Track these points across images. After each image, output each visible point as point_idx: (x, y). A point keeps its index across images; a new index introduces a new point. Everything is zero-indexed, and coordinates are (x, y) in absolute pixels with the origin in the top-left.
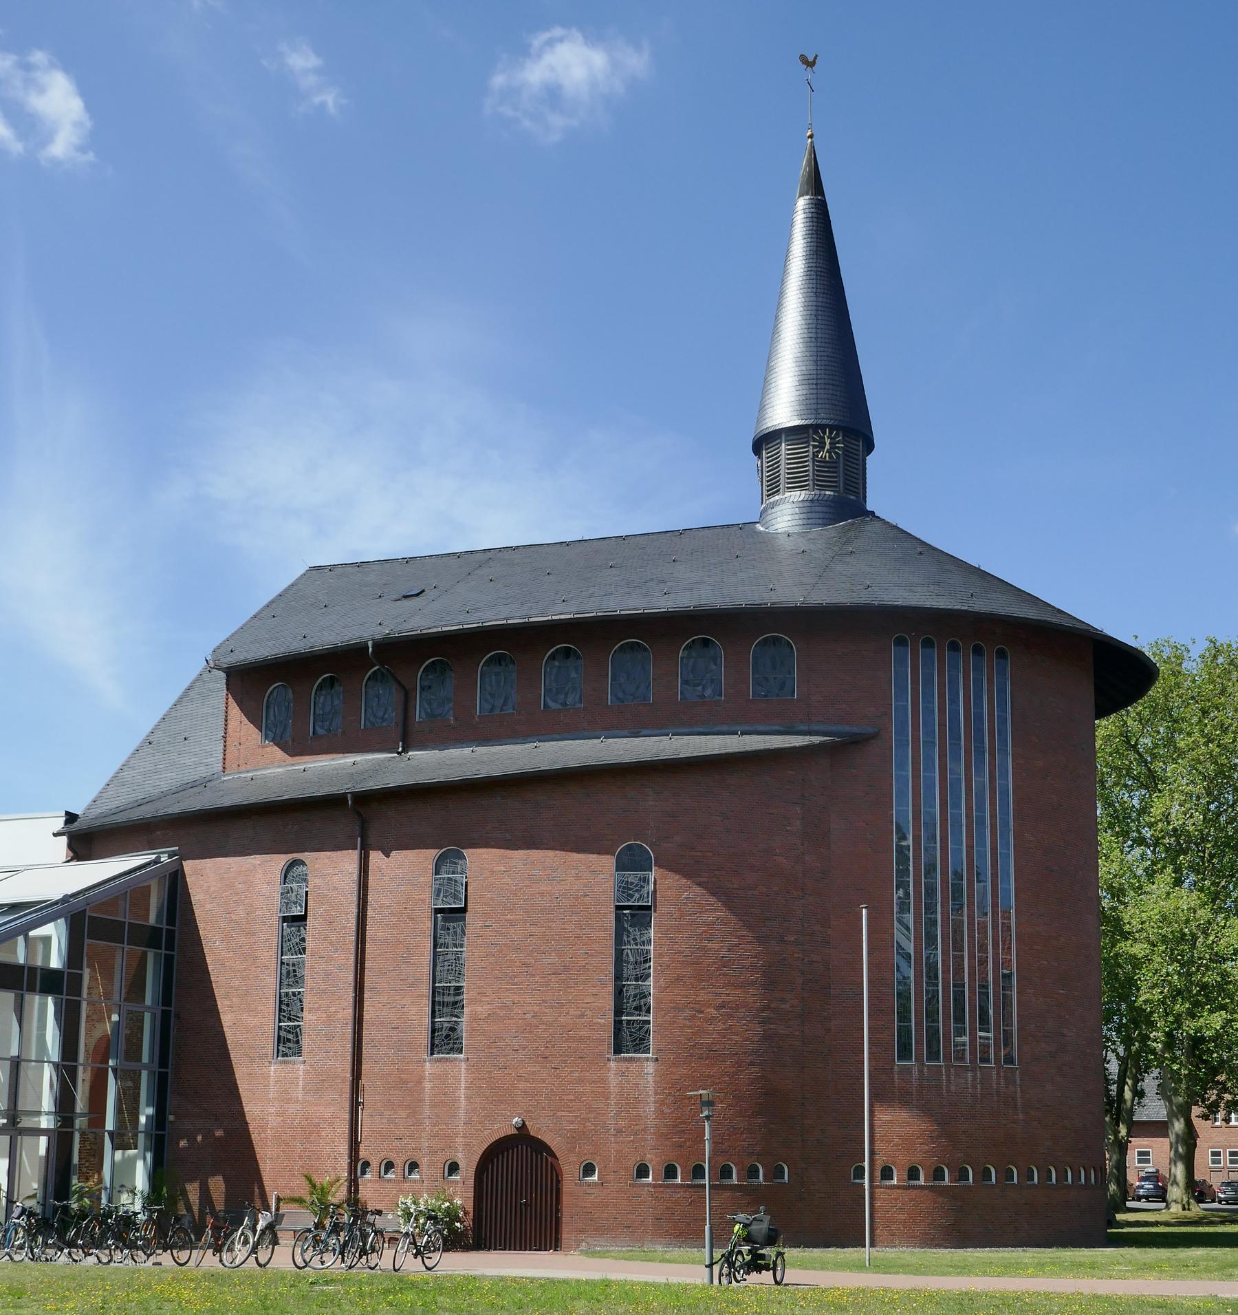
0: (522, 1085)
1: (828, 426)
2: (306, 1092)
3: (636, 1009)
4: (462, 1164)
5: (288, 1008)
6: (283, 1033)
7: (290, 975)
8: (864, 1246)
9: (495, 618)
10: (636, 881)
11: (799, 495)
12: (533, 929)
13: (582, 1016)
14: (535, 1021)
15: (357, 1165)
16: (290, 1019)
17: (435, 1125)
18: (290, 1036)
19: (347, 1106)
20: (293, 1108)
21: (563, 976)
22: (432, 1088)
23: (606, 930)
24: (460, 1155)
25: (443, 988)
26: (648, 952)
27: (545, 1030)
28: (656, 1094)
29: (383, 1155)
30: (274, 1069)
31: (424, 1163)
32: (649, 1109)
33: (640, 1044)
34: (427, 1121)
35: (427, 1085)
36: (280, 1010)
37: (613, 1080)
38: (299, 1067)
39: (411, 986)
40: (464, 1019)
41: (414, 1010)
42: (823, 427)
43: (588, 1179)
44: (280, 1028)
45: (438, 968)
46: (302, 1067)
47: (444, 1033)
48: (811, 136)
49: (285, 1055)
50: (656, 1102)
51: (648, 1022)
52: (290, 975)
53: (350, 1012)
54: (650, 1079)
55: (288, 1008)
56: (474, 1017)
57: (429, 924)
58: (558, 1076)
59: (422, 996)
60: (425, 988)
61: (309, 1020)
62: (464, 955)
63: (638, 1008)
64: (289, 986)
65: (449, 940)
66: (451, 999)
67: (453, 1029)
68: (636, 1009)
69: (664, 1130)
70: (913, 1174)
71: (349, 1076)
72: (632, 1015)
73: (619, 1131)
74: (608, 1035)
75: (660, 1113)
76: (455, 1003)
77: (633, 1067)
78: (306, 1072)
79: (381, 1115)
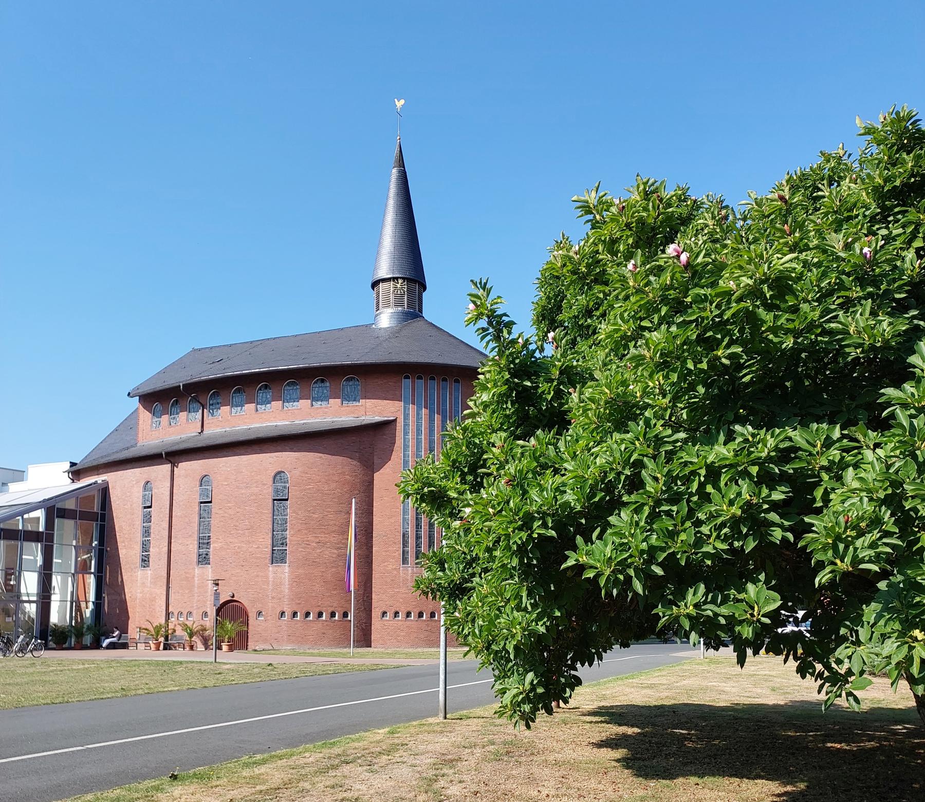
0: (233, 578)
1: (400, 278)
2: (151, 583)
3: (281, 544)
4: (209, 614)
5: (145, 547)
6: (144, 558)
7: (147, 532)
8: (439, 646)
9: (257, 367)
10: (281, 488)
11: (390, 311)
12: (238, 510)
13: (258, 547)
14: (239, 550)
15: (168, 615)
16: (146, 551)
17: (199, 596)
18: (146, 559)
19: (165, 588)
20: (146, 590)
21: (250, 530)
22: (198, 580)
23: (268, 510)
24: (208, 609)
25: (203, 536)
26: (287, 519)
27: (243, 554)
28: (289, 581)
29: (179, 610)
30: (140, 573)
31: (194, 612)
32: (286, 590)
33: (283, 560)
34: (196, 595)
35: (196, 579)
36: (143, 547)
37: (271, 575)
38: (149, 572)
39: (190, 536)
40: (211, 550)
41: (191, 546)
42: (397, 278)
43: (308, 619)
44: (143, 555)
45: (201, 528)
46: (149, 572)
47: (204, 556)
48: (400, 139)
49: (144, 567)
50: (289, 585)
51: (286, 550)
52: (147, 532)
53: (166, 548)
54: (287, 574)
55: (145, 547)
56: (215, 549)
57: (197, 509)
58: (248, 574)
59: (195, 540)
60: (196, 537)
61: (153, 552)
62: (212, 522)
63: (282, 544)
64: (146, 537)
65: (206, 516)
66: (206, 541)
67: (207, 554)
68: (281, 544)
69: (292, 597)
70: (333, 615)
71: (166, 575)
72: (280, 547)
73: (273, 598)
74: (269, 556)
75: (290, 589)
76: (208, 543)
77: (279, 569)
78: (151, 574)
79: (178, 592)
